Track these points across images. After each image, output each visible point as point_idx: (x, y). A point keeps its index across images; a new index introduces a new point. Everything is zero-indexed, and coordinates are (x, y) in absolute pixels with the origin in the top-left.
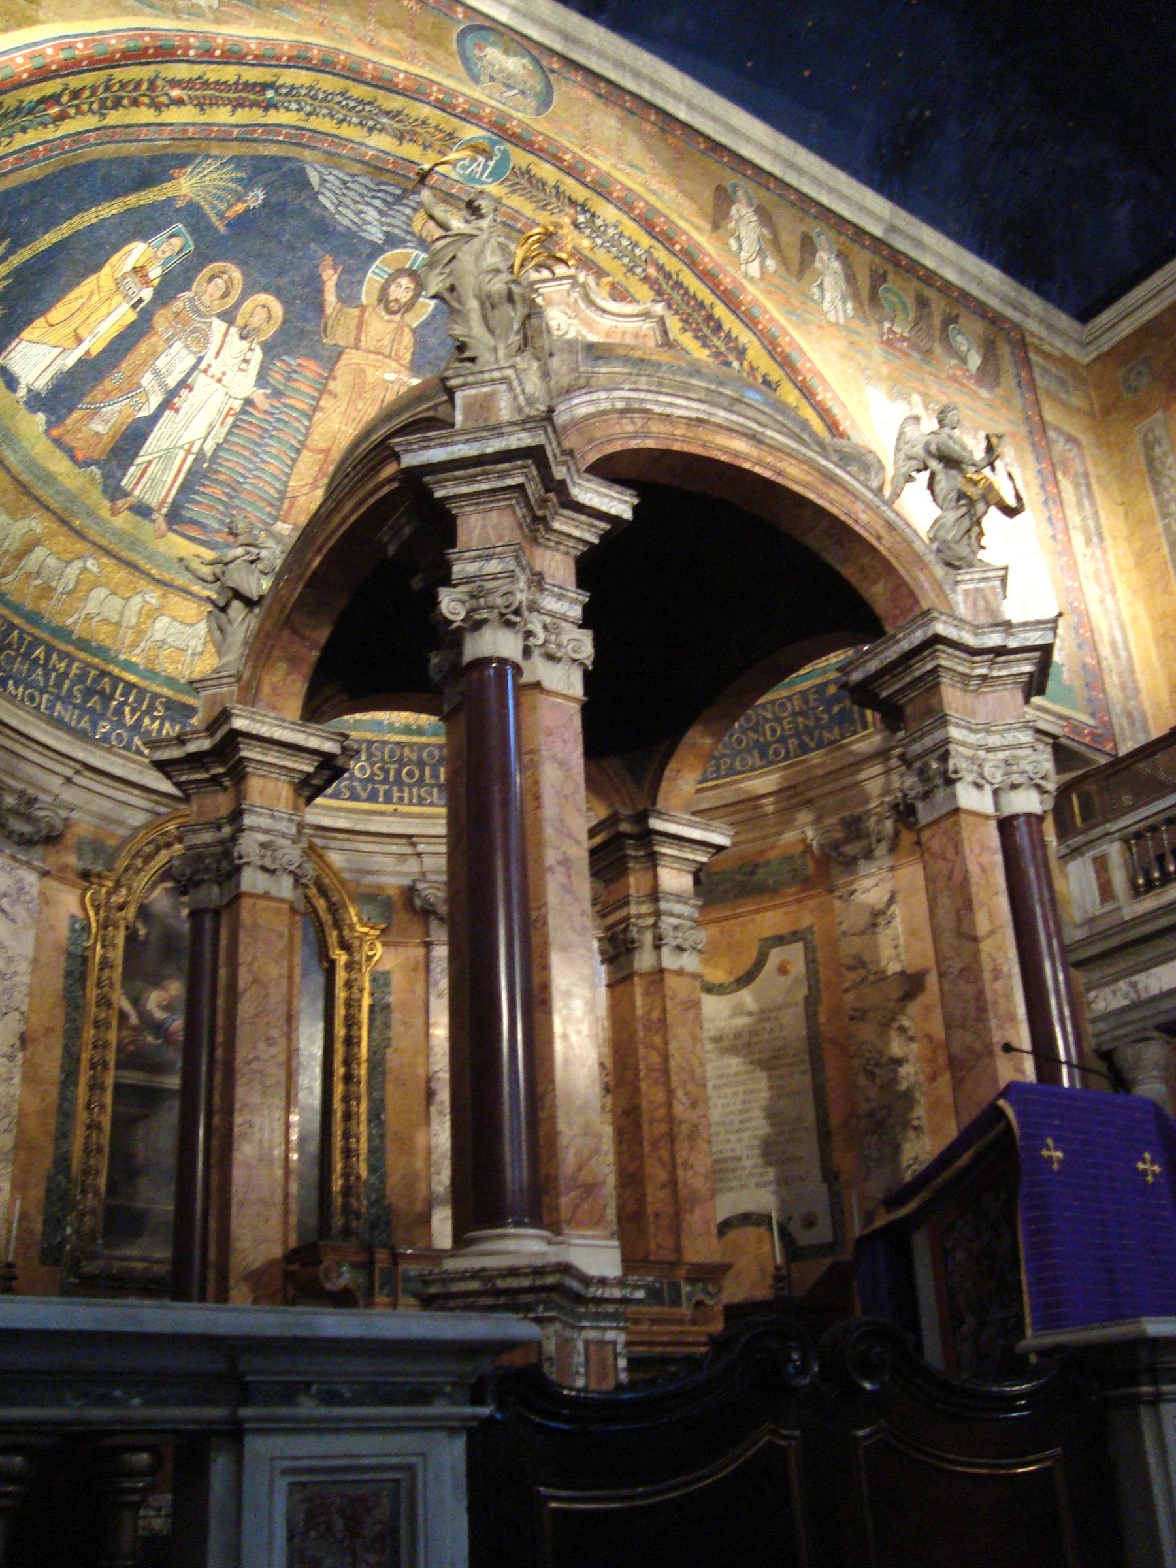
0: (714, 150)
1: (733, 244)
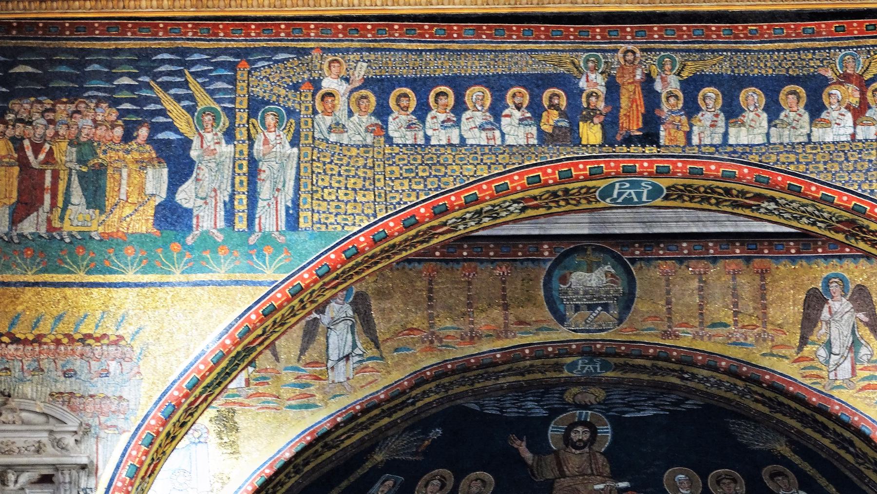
0: (807, 246)
1: (823, 353)
